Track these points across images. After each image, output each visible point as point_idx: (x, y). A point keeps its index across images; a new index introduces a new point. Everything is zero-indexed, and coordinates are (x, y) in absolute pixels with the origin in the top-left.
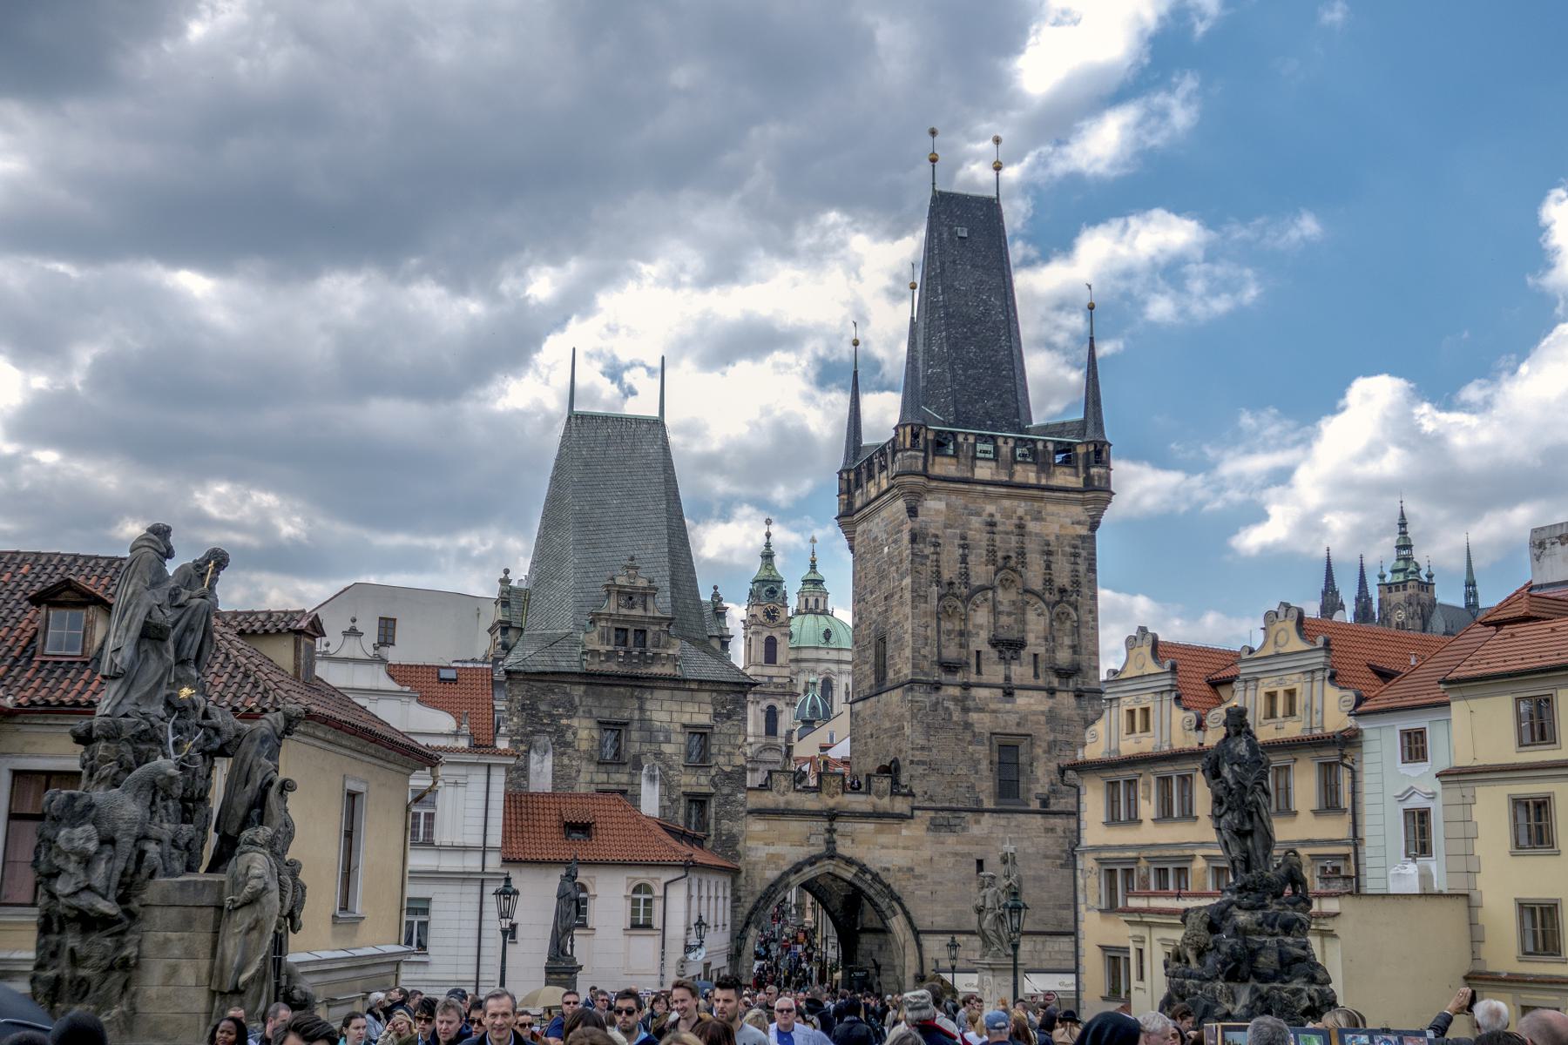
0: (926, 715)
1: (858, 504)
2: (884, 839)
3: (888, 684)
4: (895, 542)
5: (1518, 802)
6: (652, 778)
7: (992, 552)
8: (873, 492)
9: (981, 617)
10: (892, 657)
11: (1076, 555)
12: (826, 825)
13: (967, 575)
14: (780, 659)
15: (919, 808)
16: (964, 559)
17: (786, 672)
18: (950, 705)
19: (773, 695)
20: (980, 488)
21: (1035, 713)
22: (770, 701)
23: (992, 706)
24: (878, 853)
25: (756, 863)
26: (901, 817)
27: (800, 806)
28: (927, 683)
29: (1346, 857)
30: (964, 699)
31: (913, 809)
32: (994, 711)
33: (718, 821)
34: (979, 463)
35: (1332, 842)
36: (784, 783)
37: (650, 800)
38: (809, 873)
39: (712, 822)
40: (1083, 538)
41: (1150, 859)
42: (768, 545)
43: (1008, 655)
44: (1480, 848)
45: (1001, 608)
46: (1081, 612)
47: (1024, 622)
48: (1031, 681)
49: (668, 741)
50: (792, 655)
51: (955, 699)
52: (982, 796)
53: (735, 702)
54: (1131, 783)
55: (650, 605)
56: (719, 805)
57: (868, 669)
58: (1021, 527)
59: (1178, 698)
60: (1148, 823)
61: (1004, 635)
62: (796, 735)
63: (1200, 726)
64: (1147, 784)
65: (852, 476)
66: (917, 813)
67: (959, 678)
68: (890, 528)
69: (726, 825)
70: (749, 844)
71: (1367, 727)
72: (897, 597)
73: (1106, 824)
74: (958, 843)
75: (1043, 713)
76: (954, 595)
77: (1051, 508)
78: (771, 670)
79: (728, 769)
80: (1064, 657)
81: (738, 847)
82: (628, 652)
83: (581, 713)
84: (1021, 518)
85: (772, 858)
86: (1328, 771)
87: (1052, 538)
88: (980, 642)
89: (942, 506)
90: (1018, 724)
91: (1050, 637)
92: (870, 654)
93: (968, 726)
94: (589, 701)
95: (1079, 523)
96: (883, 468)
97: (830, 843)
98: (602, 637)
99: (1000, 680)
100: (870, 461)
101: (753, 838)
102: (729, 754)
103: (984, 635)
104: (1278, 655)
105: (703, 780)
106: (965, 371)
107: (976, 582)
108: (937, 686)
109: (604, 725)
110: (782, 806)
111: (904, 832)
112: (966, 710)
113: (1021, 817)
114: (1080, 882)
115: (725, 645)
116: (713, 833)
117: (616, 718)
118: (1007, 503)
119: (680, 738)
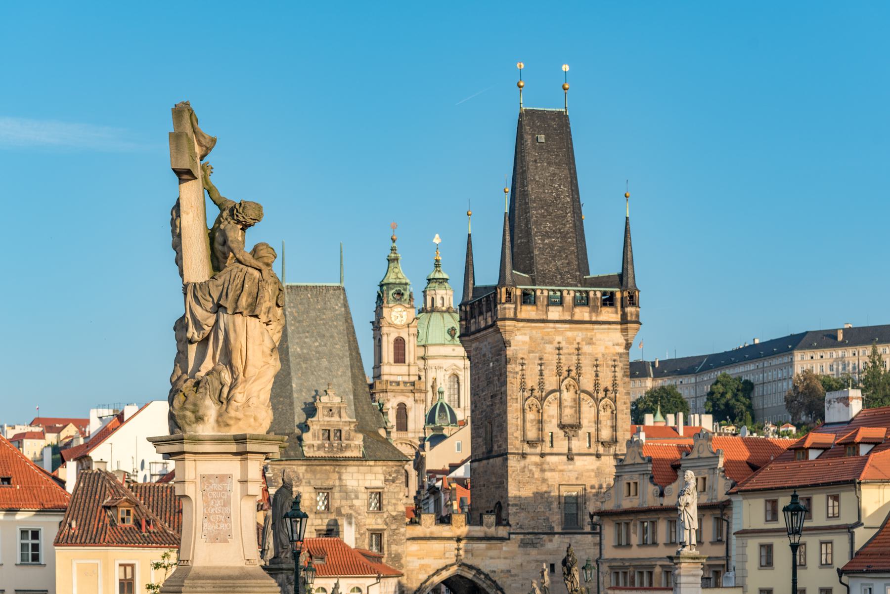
0: (518, 475)
1: (473, 329)
2: (492, 553)
3: (494, 453)
4: (497, 360)
5: (762, 546)
6: (350, 523)
7: (559, 367)
8: (483, 325)
9: (551, 410)
10: (496, 436)
11: (615, 366)
13: (541, 384)
14: (410, 357)
15: (513, 533)
16: (541, 375)
17: (414, 370)
18: (533, 468)
19: (402, 392)
20: (551, 325)
21: (588, 471)
22: (401, 399)
23: (560, 468)
24: (488, 562)
25: (413, 570)
26: (502, 539)
27: (439, 535)
28: (518, 454)
29: (723, 566)
30: (542, 464)
31: (510, 534)
32: (561, 471)
33: (389, 545)
34: (551, 308)
35: (717, 558)
37: (349, 536)
38: (445, 575)
40: (621, 355)
41: (635, 567)
42: (393, 249)
43: (571, 434)
44: (748, 566)
45: (565, 404)
46: (618, 403)
47: (579, 412)
48: (587, 451)
49: (357, 498)
50: (421, 352)
51: (536, 464)
52: (553, 525)
53: (397, 472)
54: (627, 524)
55: (343, 414)
56: (389, 536)
57: (480, 440)
58: (578, 349)
59: (652, 478)
60: (635, 548)
61: (567, 420)
62: (427, 444)
63: (662, 494)
64: (635, 525)
65: (468, 309)
66: (512, 536)
67: (538, 450)
68: (493, 350)
70: (409, 559)
71: (734, 499)
72: (498, 397)
73: (615, 547)
74: (538, 554)
75: (593, 470)
76: (535, 397)
77: (599, 336)
78: (402, 369)
79: (394, 514)
80: (606, 434)
82: (331, 445)
83: (304, 483)
84: (578, 343)
85: (423, 567)
86: (719, 520)
87: (600, 356)
88: (551, 426)
89: (526, 338)
90: (577, 478)
91: (598, 422)
92: (482, 431)
93: (544, 480)
94: (308, 476)
95: (618, 345)
96: (489, 310)
97: (457, 556)
98: (314, 436)
99: (566, 451)
100: (480, 301)
102: (395, 504)
103: (555, 422)
104: (699, 458)
106: (543, 240)
107: (548, 387)
108: (524, 456)
109: (317, 490)
110: (428, 535)
111: (504, 549)
112: (543, 471)
113: (579, 537)
114: (601, 579)
115: (388, 433)
116: (386, 553)
117: (325, 485)
118: (569, 334)
119: (364, 496)
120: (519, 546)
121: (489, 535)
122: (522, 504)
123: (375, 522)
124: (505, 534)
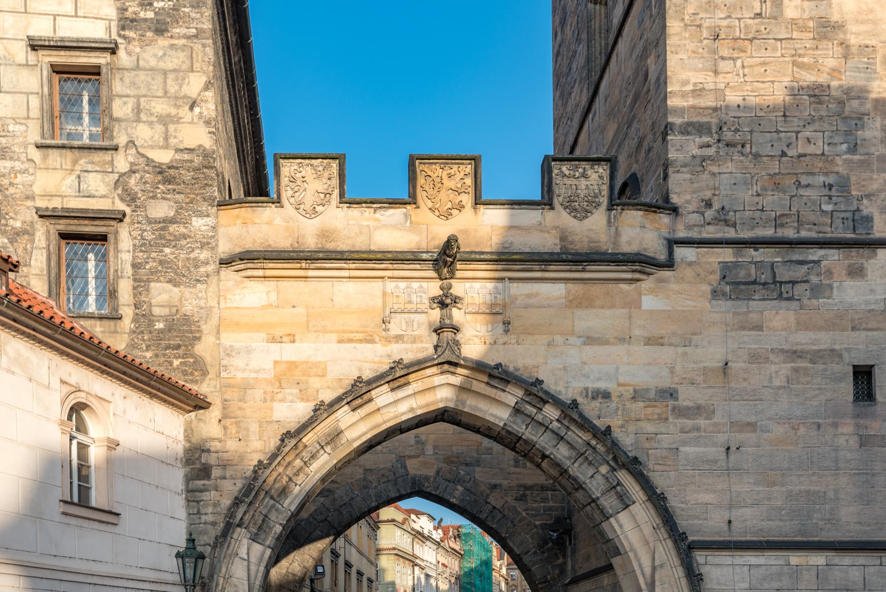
2: (592, 320)
12: (434, 288)
24: (575, 354)
27: (360, 243)
33: (140, 284)
36: (320, 186)
39: (125, 289)
56: (143, 246)
69: (162, 295)
70: (228, 339)
74: (802, 326)
81: (200, 349)
85: (289, 375)
101: (237, 326)
105: (97, 183)
110: (311, 243)
111: (649, 302)
116: (127, 313)
120: (715, 294)
121: (581, 245)
122: (727, 131)
123: (87, 187)
124: (654, 247)
